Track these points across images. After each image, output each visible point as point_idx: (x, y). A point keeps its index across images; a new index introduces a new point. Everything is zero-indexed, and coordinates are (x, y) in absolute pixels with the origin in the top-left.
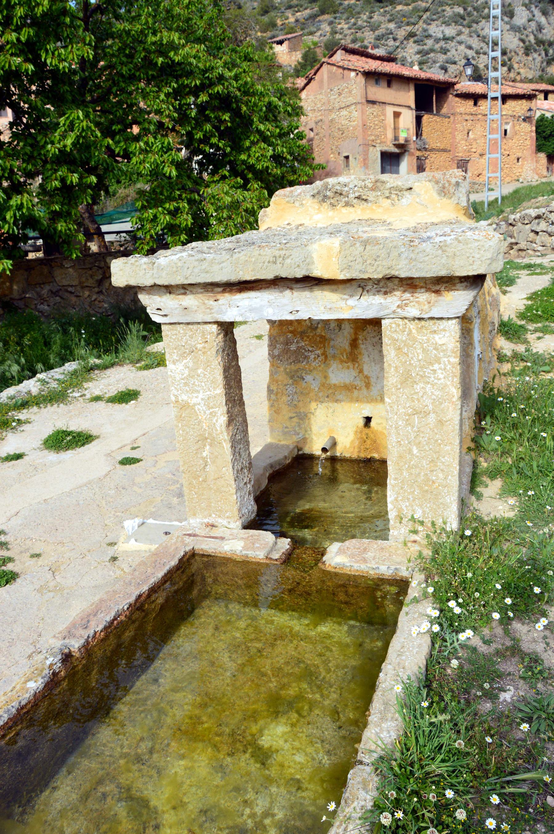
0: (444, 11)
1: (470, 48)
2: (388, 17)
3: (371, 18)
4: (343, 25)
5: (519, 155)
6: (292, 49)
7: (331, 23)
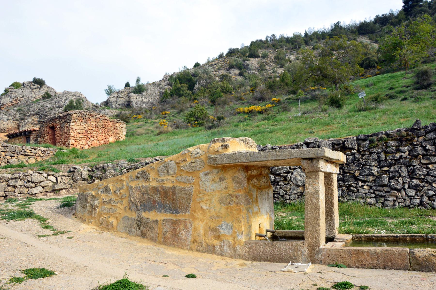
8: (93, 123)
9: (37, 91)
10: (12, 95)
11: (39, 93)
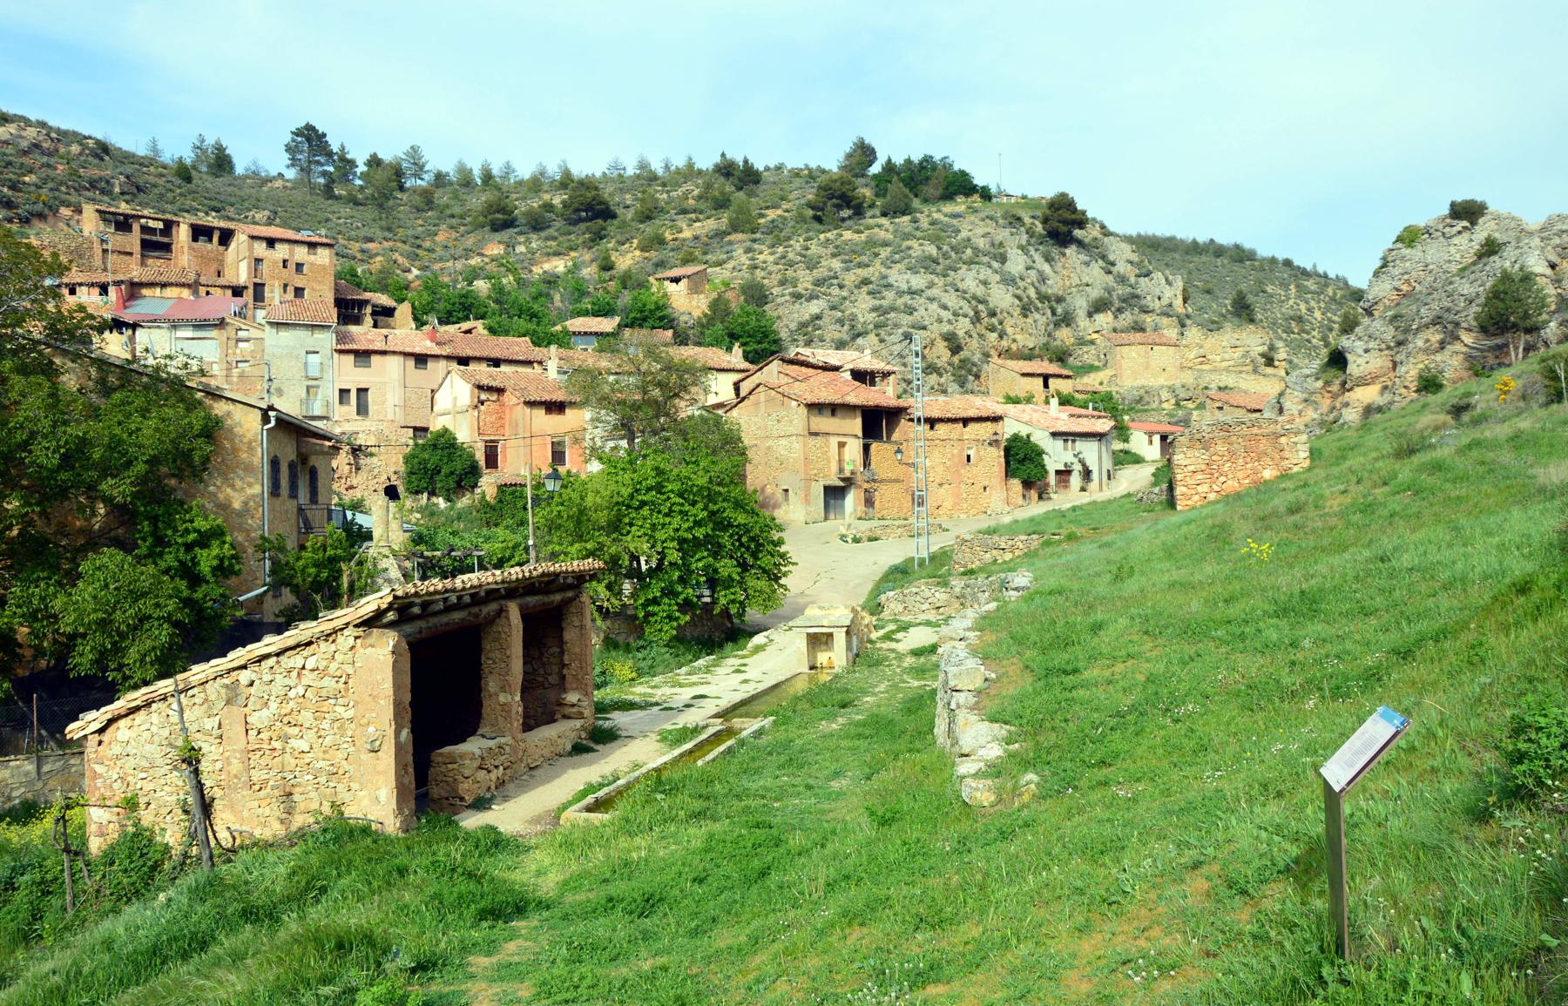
0: (909, 248)
1: (945, 308)
2: (831, 249)
3: (807, 249)
4: (766, 256)
5: (986, 483)
6: (695, 289)
7: (748, 250)
8: (1221, 448)
9: (1462, 241)
10: (1396, 272)
11: (1466, 244)
